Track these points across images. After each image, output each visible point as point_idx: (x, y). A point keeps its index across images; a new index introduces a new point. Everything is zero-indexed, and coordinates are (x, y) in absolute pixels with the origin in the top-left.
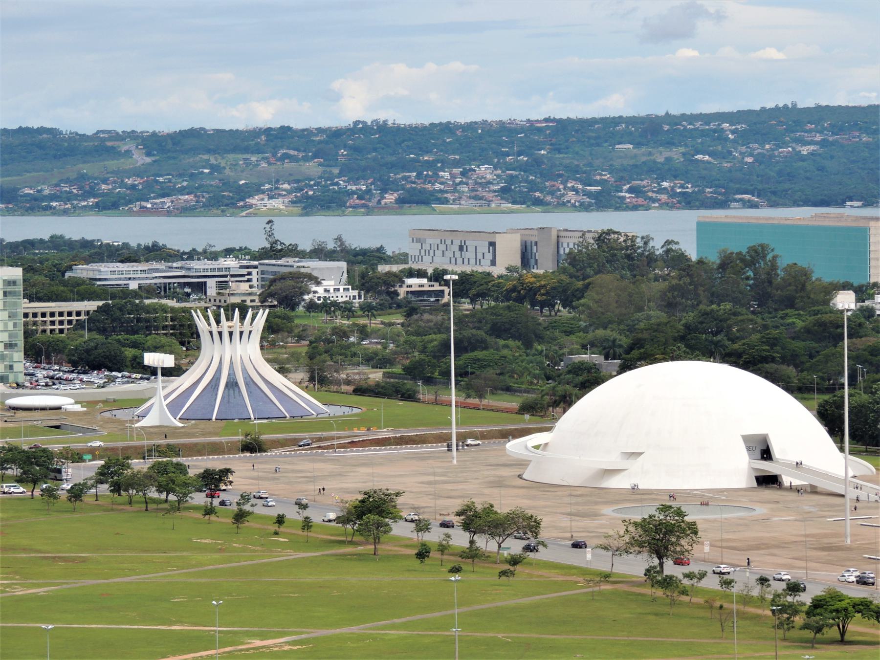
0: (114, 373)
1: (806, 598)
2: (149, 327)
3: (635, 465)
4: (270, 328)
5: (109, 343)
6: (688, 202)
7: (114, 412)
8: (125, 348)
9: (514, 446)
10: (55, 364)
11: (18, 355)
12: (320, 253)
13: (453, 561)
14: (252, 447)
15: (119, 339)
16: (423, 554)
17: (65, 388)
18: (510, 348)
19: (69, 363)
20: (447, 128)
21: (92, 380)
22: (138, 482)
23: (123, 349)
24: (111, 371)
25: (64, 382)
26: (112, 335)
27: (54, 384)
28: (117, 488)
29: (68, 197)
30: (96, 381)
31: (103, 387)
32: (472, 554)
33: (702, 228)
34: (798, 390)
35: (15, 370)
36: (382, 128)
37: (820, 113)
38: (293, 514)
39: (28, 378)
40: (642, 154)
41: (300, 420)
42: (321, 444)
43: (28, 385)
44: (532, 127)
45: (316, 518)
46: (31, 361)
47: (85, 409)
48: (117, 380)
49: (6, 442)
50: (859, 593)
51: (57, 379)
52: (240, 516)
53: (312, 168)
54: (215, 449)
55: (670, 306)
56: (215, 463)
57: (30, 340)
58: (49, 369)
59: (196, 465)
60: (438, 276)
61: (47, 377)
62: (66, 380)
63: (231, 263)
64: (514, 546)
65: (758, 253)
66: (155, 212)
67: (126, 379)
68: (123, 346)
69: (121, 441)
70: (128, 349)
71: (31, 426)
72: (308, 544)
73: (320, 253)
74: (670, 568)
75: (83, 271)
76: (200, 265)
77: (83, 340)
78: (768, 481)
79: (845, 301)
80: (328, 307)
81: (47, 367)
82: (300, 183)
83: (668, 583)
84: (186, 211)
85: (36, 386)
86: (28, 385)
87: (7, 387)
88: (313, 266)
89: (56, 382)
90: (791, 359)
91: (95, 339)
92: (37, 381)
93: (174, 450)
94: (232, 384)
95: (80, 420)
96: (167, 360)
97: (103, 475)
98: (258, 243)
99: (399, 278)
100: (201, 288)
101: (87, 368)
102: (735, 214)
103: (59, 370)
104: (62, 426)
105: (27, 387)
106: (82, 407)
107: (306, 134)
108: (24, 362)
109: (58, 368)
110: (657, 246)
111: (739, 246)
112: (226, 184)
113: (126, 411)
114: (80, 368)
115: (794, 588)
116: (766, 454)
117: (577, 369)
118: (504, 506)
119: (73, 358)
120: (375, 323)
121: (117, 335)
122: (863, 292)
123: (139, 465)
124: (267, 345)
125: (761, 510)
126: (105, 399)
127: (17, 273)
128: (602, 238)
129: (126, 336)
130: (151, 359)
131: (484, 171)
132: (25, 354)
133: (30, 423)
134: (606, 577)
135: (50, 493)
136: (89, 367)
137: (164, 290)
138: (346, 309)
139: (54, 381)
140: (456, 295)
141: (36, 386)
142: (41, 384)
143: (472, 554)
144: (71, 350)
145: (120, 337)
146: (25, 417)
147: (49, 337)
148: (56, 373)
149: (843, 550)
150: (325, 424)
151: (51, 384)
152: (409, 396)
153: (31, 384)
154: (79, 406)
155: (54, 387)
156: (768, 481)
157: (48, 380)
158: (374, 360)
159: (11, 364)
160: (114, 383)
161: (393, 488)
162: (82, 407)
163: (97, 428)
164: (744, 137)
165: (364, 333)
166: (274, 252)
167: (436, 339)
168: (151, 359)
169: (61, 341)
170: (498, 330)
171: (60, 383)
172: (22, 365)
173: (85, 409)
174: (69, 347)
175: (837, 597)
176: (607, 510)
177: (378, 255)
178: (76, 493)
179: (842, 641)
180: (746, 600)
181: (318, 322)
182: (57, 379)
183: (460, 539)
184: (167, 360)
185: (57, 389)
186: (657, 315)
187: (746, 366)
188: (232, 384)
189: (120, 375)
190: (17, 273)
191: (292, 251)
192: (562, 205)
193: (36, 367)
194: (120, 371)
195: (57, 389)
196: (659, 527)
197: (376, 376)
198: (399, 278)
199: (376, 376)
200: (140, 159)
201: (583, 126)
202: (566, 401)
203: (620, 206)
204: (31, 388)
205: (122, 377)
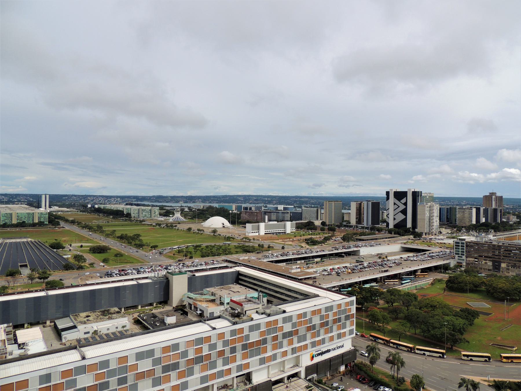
1: (227, 237)
2: (170, 213)
3: (213, 225)
4: (181, 213)
6: (217, 203)
9: (202, 224)
11: (159, 215)
12: (185, 207)
13: (196, 233)
14: (179, 223)
16: (194, 233)
18: (202, 215)
20: (197, 196)
22: (169, 226)
28: (167, 227)
29: (163, 201)
32: (198, 233)
33: (218, 205)
34: (226, 219)
36: (191, 196)
37: (229, 196)
38: (182, 229)
40: (214, 199)
41: (183, 221)
42: (185, 223)
44: (204, 196)
45: (185, 230)
50: (231, 236)
52: (178, 229)
53: (185, 199)
54: (176, 224)
55: (216, 212)
56: (176, 225)
59: (174, 225)
60: (196, 209)
63: (177, 207)
64: (202, 232)
65: (223, 207)
66: (171, 203)
72: (183, 232)
73: (185, 207)
74: (215, 234)
75: (164, 208)
76: (175, 207)
78: (224, 227)
79: (231, 212)
80: (186, 211)
82: (184, 201)
83: (215, 235)
84: (174, 203)
88: (185, 208)
90: (226, 216)
93: (172, 224)
94: (177, 218)
96: (172, 216)
97: (166, 226)
98: (180, 206)
99: (192, 209)
100: (175, 209)
102: (221, 204)
107: (184, 196)
110: (215, 207)
111: (222, 207)
112: (178, 201)
115: (226, 236)
116: (224, 225)
117: (208, 217)
118: (201, 229)
120: (190, 213)
122: (232, 211)
123: (169, 225)
124: (181, 214)
125: (223, 229)
127: (159, 208)
128: (210, 206)
130: (170, 216)
131: (200, 200)
134: (210, 235)
135: (161, 227)
137: (172, 210)
138: (188, 212)
140: (197, 210)
143: (198, 233)
150: (185, 222)
152: (193, 219)
156: (224, 227)
158: (190, 216)
161: (191, 227)
164: (222, 198)
165: (189, 214)
166: (181, 206)
167: (195, 214)
168: (170, 216)
170: (201, 214)
175: (229, 237)
176: (210, 229)
177: (191, 207)
178: (163, 227)
179: (230, 240)
180: (222, 237)
181: (185, 213)
183: (197, 232)
184: (172, 216)
186: (214, 212)
187: (222, 217)
188: (177, 218)
190: (159, 208)
191: (183, 206)
192: (207, 203)
196: (214, 231)
197: (190, 217)
198: (192, 209)
199: (190, 217)
200: (170, 198)
201: (208, 196)
202: (207, 220)
203: (212, 203)
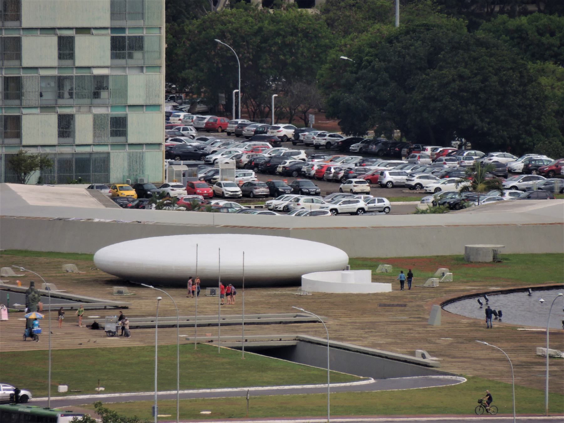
0: (497, 157)
5: (480, 43)
7: (496, 303)
8: (539, 65)
10: (280, 118)
15: (519, 30)
17: (316, 207)
19: (330, 116)
21: (416, 180)
23: (532, 67)
24: (488, 149)
25: (312, 186)
26: (491, 14)
27: (275, 193)
30: (431, 184)
31: (455, 206)
35: (132, 138)
39: (181, 167)
43: (181, 193)
46: (193, 104)
47: (386, 288)
48: (509, 183)
49: (98, 404)
51: (287, 173)
57: (191, 26)
58: (257, 136)
61: (250, 166)
62: (319, 177)
67: (542, 181)
68: (534, 57)
69: (315, 368)
70: (550, 65)
71: (187, 347)
77: (385, 29)
81: (251, 128)
85: (209, 197)
86: (181, 193)
87: (101, 200)
89: (283, 183)
91: (428, 27)
92: (209, 180)
95: (371, 327)
101: (397, 133)
103: (296, 142)
104: (304, 349)
105: (175, 201)
106: (375, 279)
108: (167, 107)
109: (290, 133)
113: (541, 297)
114: (370, 135)
119: (348, 98)
121: (512, 15)
126: (461, 252)
129: (544, 20)
132: (169, 78)
133: (183, 335)
136: (405, 132)
139: (275, 180)
141: (209, 197)
142: (228, 190)
144: (338, 65)
145: (524, 20)
146: (165, 313)
147: (259, 18)
148: (284, 150)
149: (270, 324)
151: (263, 190)
153: (191, 189)
154: (367, 274)
155: (274, 202)
157: (251, 176)
159: (119, 113)
160: (495, 194)
162: (375, 279)
163: (430, 360)
169: (306, 35)
171: (298, 190)
172: (159, 118)
173: (386, 288)
174: (332, 54)
182: (287, 173)
185: (287, 210)
189: (518, 164)
193: (209, 129)
194: (518, 152)
195: (287, 210)
204: (191, 207)
205: (527, 170)
